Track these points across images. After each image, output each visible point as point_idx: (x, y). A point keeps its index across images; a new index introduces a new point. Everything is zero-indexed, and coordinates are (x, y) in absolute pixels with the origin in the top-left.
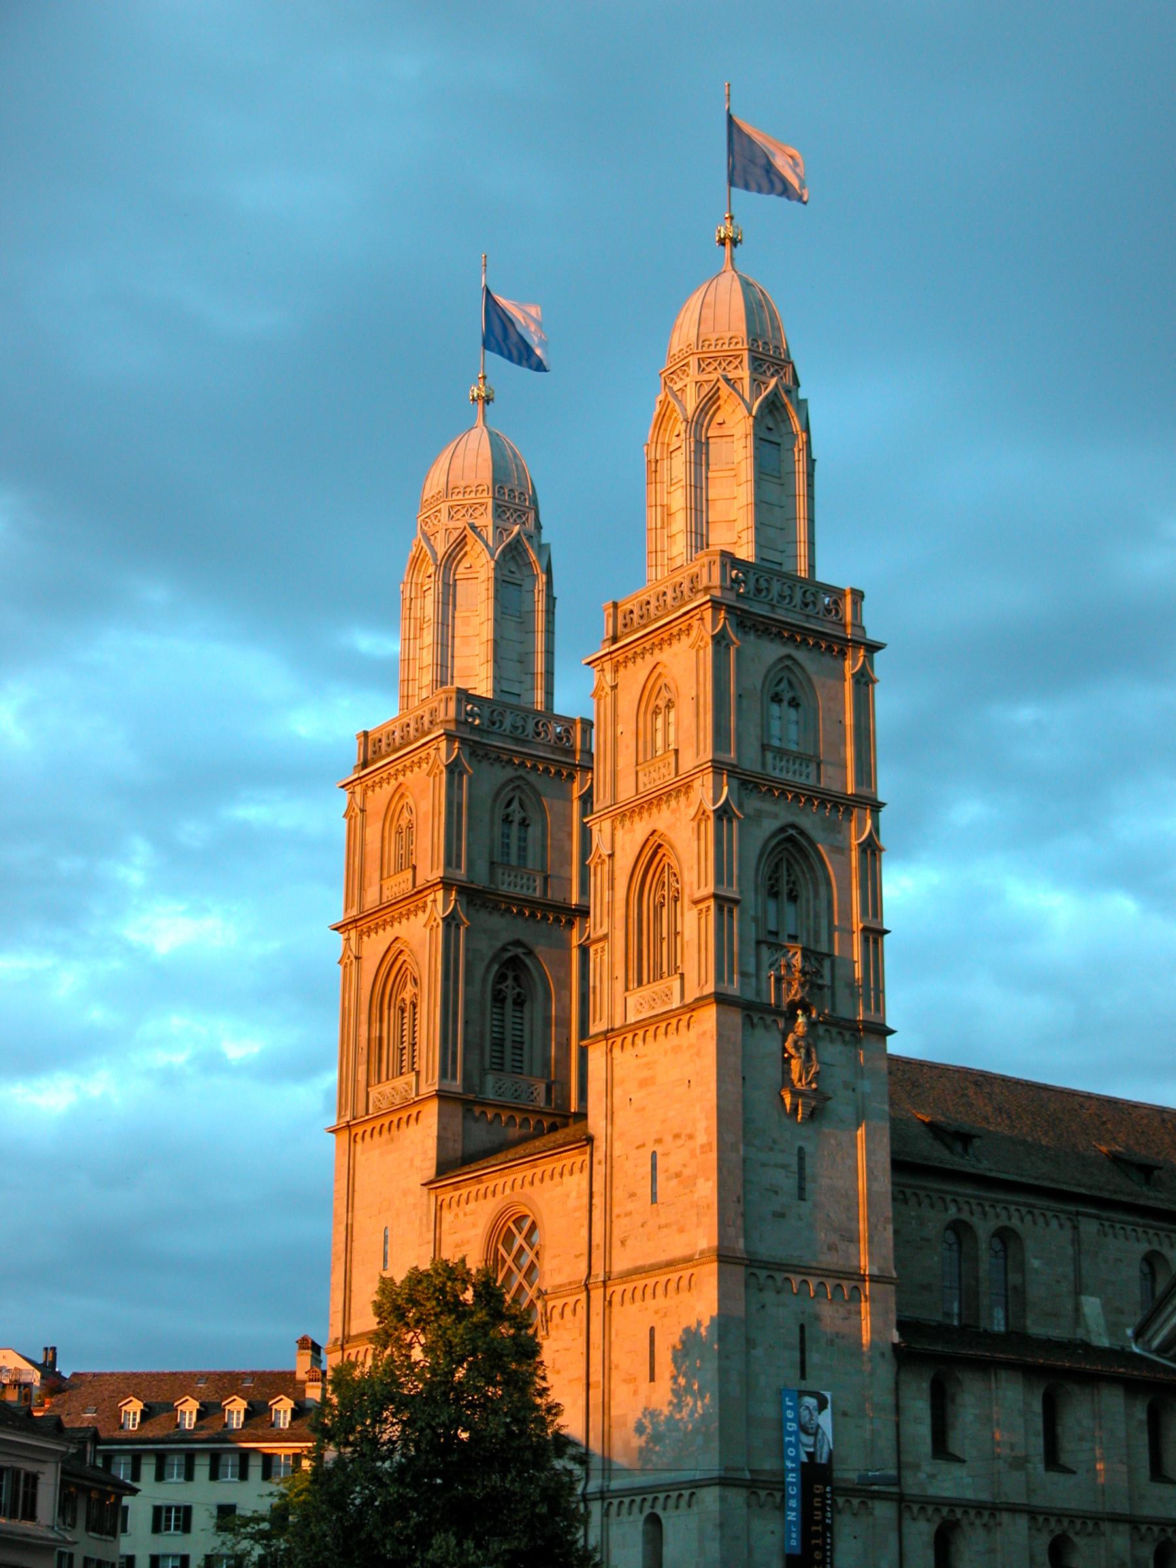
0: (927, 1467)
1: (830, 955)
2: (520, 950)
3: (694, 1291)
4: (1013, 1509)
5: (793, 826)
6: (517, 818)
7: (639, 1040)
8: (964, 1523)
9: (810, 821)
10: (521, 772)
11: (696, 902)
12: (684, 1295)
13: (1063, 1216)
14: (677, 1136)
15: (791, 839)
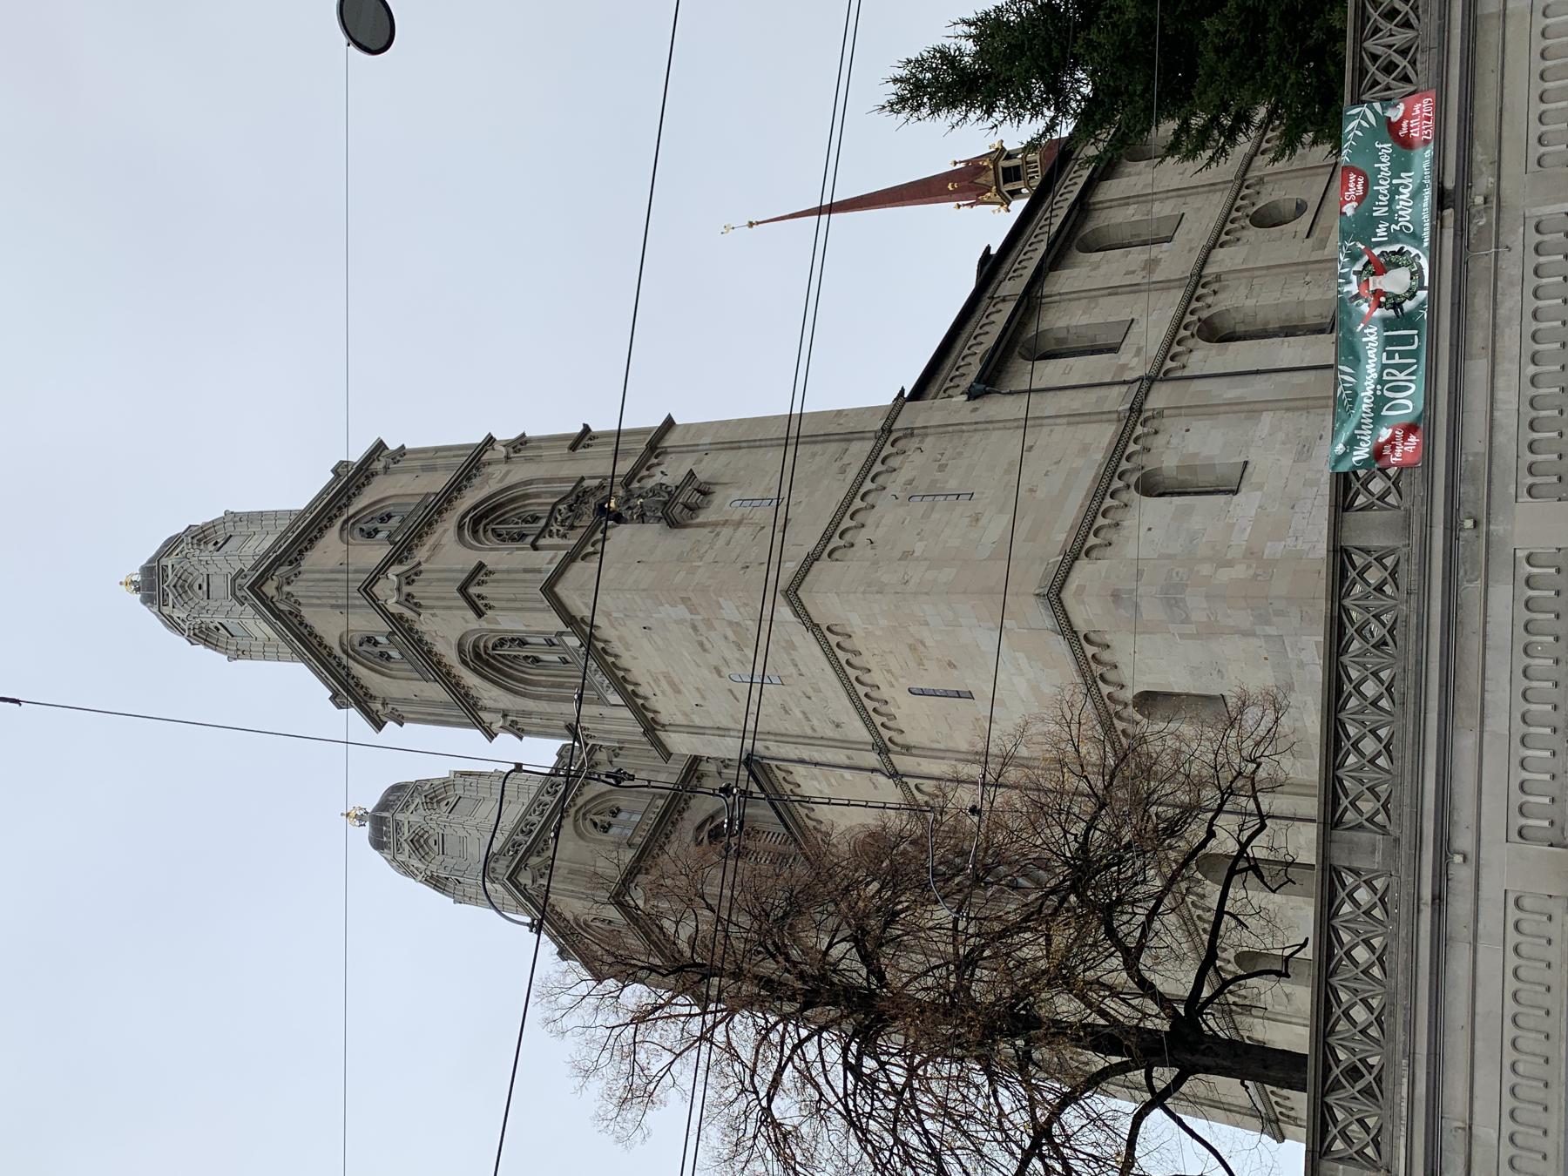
0: (1126, 356)
1: (583, 479)
2: (708, 827)
3: (849, 630)
4: (1204, 262)
5: (464, 517)
6: (608, 818)
7: (640, 691)
8: (1205, 314)
9: (470, 498)
10: (572, 811)
11: (480, 614)
12: (857, 643)
13: (991, 309)
14: (701, 645)
15: (476, 522)
